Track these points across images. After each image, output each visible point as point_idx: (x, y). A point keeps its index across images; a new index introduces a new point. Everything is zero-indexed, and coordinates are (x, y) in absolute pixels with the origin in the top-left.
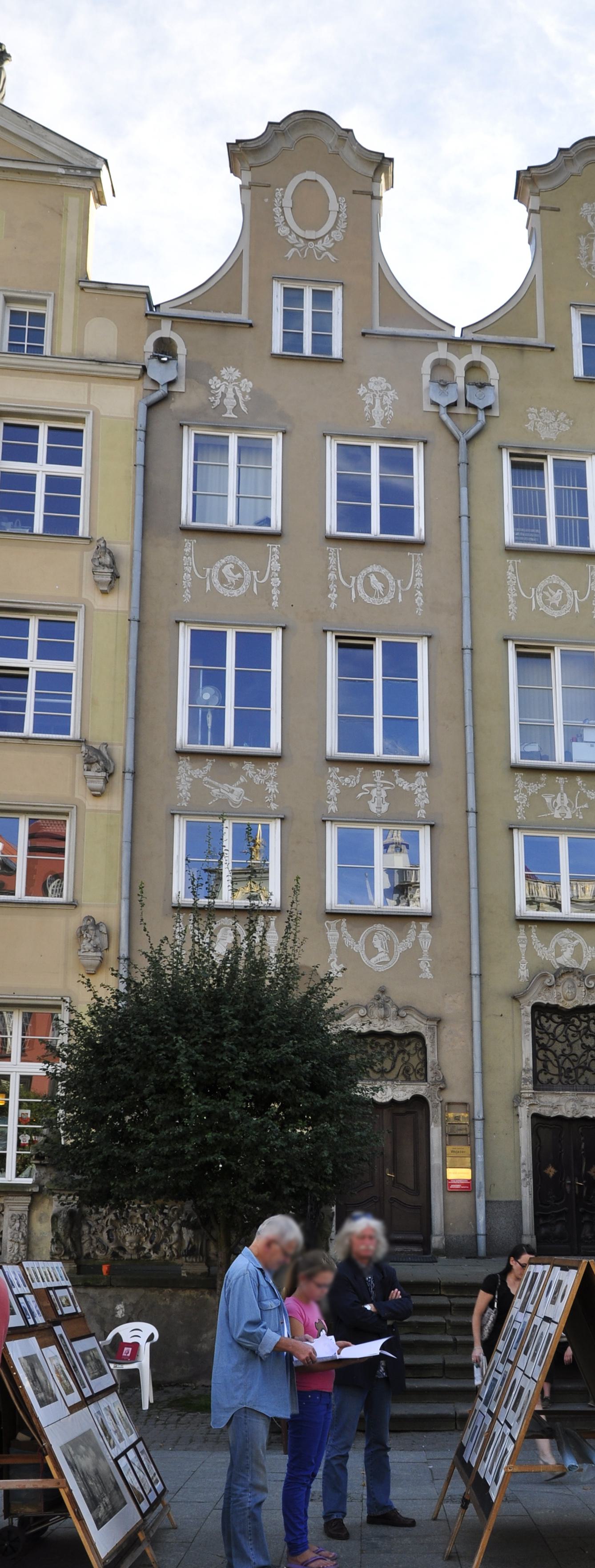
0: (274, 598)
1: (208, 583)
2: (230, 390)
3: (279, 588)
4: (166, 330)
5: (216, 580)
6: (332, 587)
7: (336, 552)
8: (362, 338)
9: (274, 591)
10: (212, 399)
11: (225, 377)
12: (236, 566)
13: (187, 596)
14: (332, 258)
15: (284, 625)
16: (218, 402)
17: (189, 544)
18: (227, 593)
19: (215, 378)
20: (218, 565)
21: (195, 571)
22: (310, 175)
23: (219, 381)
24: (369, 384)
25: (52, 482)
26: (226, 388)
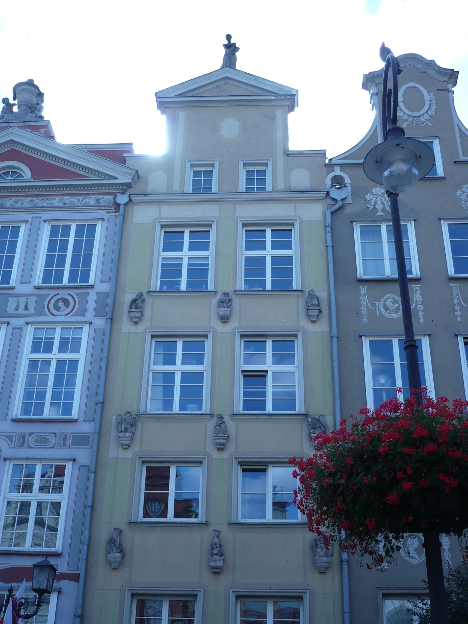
0: (420, 317)
1: (377, 311)
2: (379, 200)
3: (423, 311)
4: (337, 171)
5: (382, 309)
6: (457, 308)
7: (456, 287)
8: (455, 165)
9: (420, 313)
10: (369, 205)
11: (375, 193)
12: (394, 299)
13: (365, 320)
14: (430, 124)
15: (429, 333)
16: (372, 207)
17: (363, 289)
18: (390, 316)
19: (369, 194)
20: (383, 300)
21: (369, 304)
22: (412, 84)
23: (372, 196)
24: (463, 189)
25: (275, 260)
26: (376, 199)
